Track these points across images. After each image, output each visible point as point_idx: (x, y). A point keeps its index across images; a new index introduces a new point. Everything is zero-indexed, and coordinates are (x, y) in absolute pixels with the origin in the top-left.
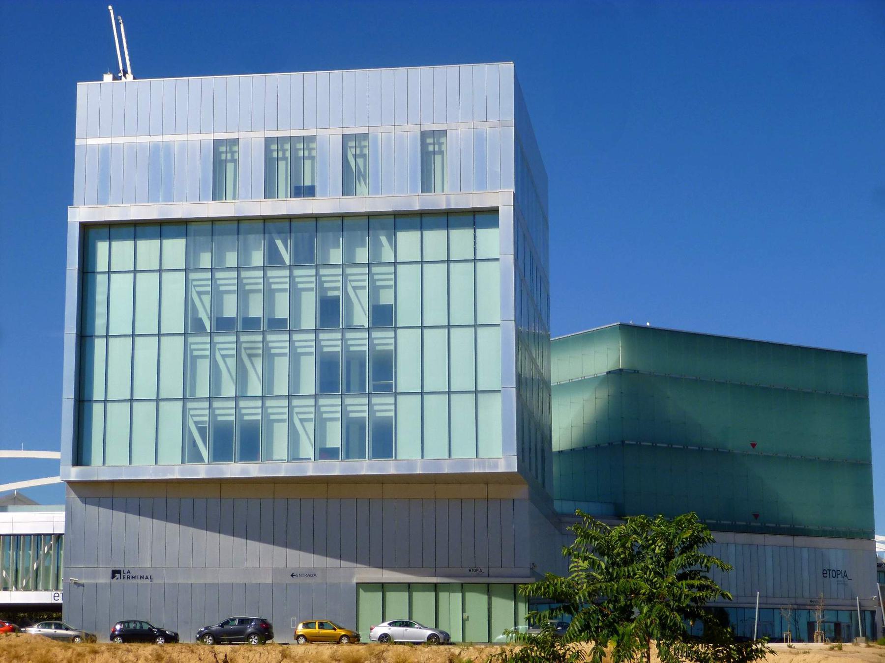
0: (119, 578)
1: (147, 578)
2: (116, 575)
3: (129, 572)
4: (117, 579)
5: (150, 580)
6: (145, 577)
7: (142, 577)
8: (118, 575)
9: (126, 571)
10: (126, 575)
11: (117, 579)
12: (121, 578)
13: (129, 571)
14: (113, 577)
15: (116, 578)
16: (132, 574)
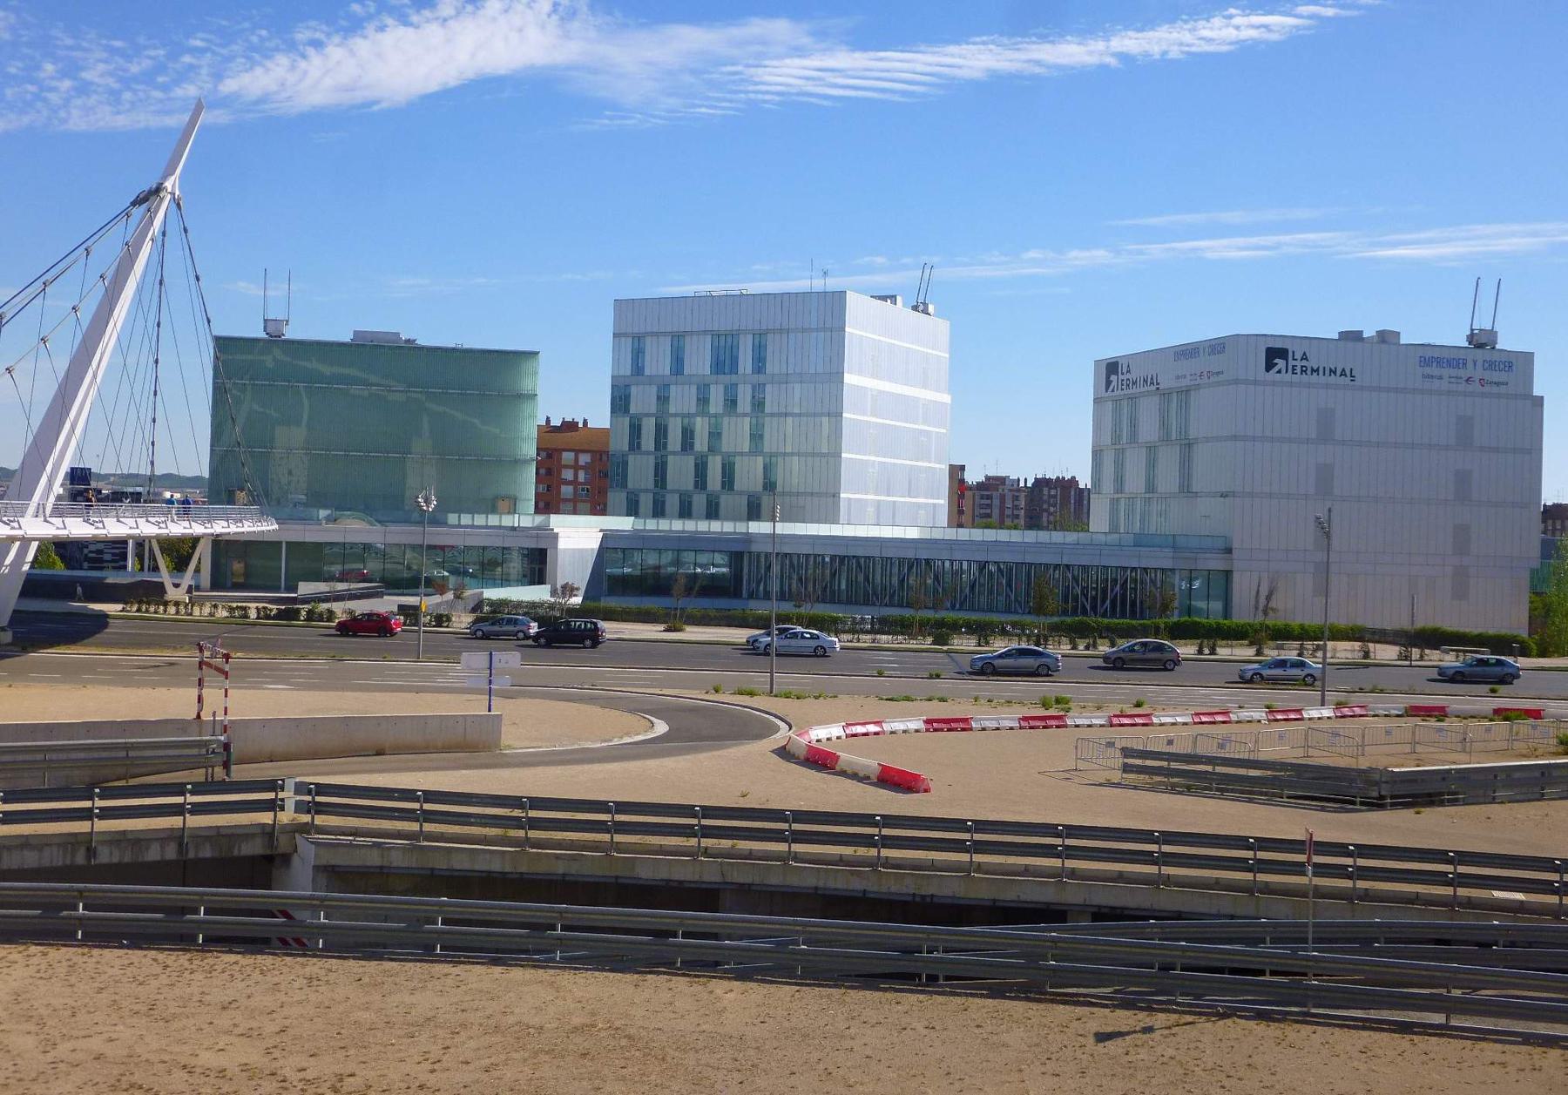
0: (1284, 370)
1: (1343, 374)
2: (1276, 361)
3: (1304, 357)
4: (1279, 372)
5: (1349, 378)
6: (1338, 373)
7: (1332, 372)
8: (1280, 363)
9: (1298, 356)
10: (1299, 364)
11: (1279, 372)
12: (1287, 372)
13: (1305, 354)
14: (1269, 366)
15: (1276, 369)
16: (1313, 363)
